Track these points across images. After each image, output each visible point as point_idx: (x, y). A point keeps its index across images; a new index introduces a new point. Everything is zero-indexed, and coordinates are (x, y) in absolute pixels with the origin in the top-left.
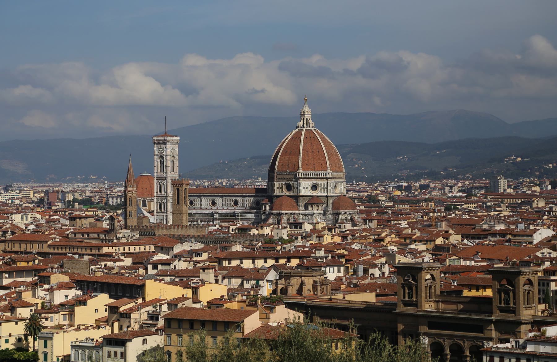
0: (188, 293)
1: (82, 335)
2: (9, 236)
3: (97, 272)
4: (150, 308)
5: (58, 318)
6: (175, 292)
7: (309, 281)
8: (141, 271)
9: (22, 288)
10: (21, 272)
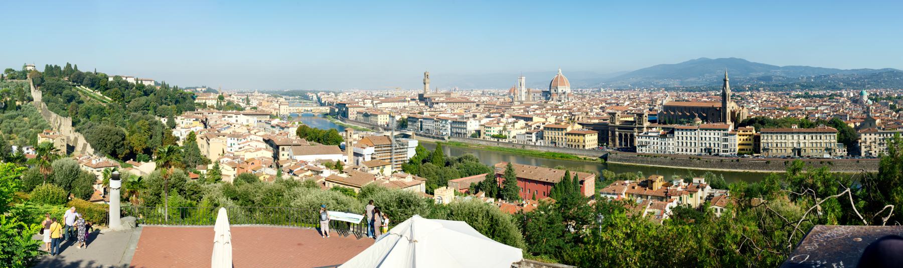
1: (519, 132)
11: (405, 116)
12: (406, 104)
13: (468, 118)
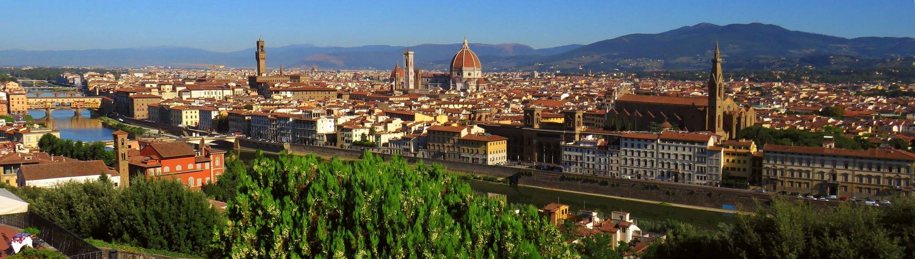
1: (392, 136)
3: (392, 108)
5: (380, 129)
6: (429, 119)
10: (362, 107)
11: (224, 111)
12: (228, 93)
13: (318, 115)
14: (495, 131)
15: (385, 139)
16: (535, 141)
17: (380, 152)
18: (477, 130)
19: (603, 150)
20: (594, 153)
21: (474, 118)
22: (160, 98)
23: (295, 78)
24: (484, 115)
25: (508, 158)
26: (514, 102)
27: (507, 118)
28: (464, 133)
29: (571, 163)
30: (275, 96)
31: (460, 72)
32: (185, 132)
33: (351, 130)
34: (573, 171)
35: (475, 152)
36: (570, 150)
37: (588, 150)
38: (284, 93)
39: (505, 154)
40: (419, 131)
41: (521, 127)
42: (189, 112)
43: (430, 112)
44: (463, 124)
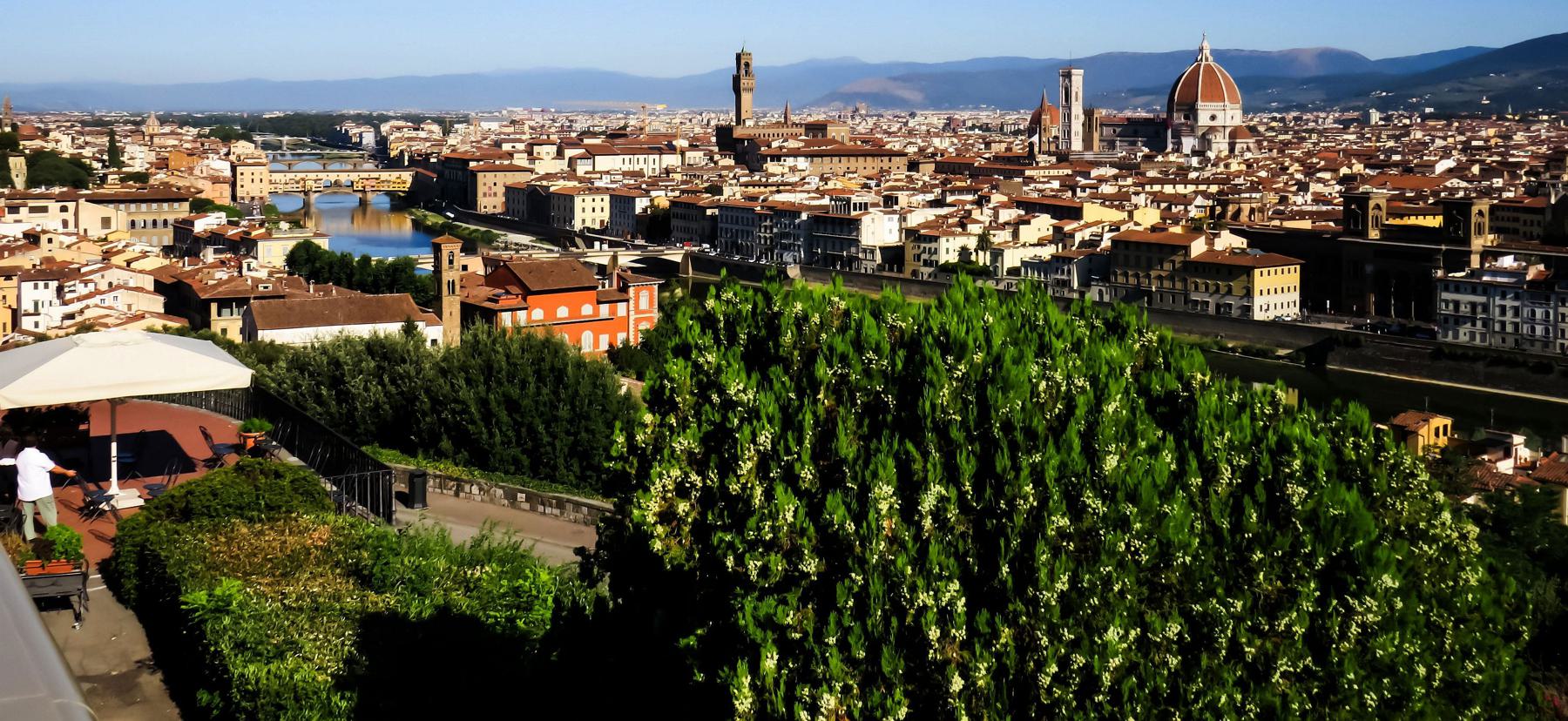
0: (1125, 215)
1: (1029, 254)
2: (938, 158)
4: (1094, 229)
6: (1116, 215)
7: (1246, 208)
8: (1069, 194)
9: (968, 207)
10: (961, 191)
11: (662, 199)
12: (671, 160)
14: (1272, 245)
15: (1012, 259)
16: (1369, 269)
17: (1001, 287)
18: (1228, 241)
19: (1538, 291)
20: (1516, 298)
21: (1223, 214)
22: (532, 171)
23: (816, 129)
24: (1246, 208)
25: (1303, 305)
26: (1320, 180)
27: (1302, 215)
28: (1198, 247)
29: (1458, 320)
30: (771, 167)
31: (1191, 113)
32: (578, 241)
33: (936, 239)
34: (1463, 338)
35: (1223, 290)
36: (1457, 291)
37: (1503, 291)
38: (790, 161)
39: (1296, 296)
40: (1092, 243)
41: (1335, 235)
42: (589, 199)
43: (1119, 200)
44: (1195, 228)
